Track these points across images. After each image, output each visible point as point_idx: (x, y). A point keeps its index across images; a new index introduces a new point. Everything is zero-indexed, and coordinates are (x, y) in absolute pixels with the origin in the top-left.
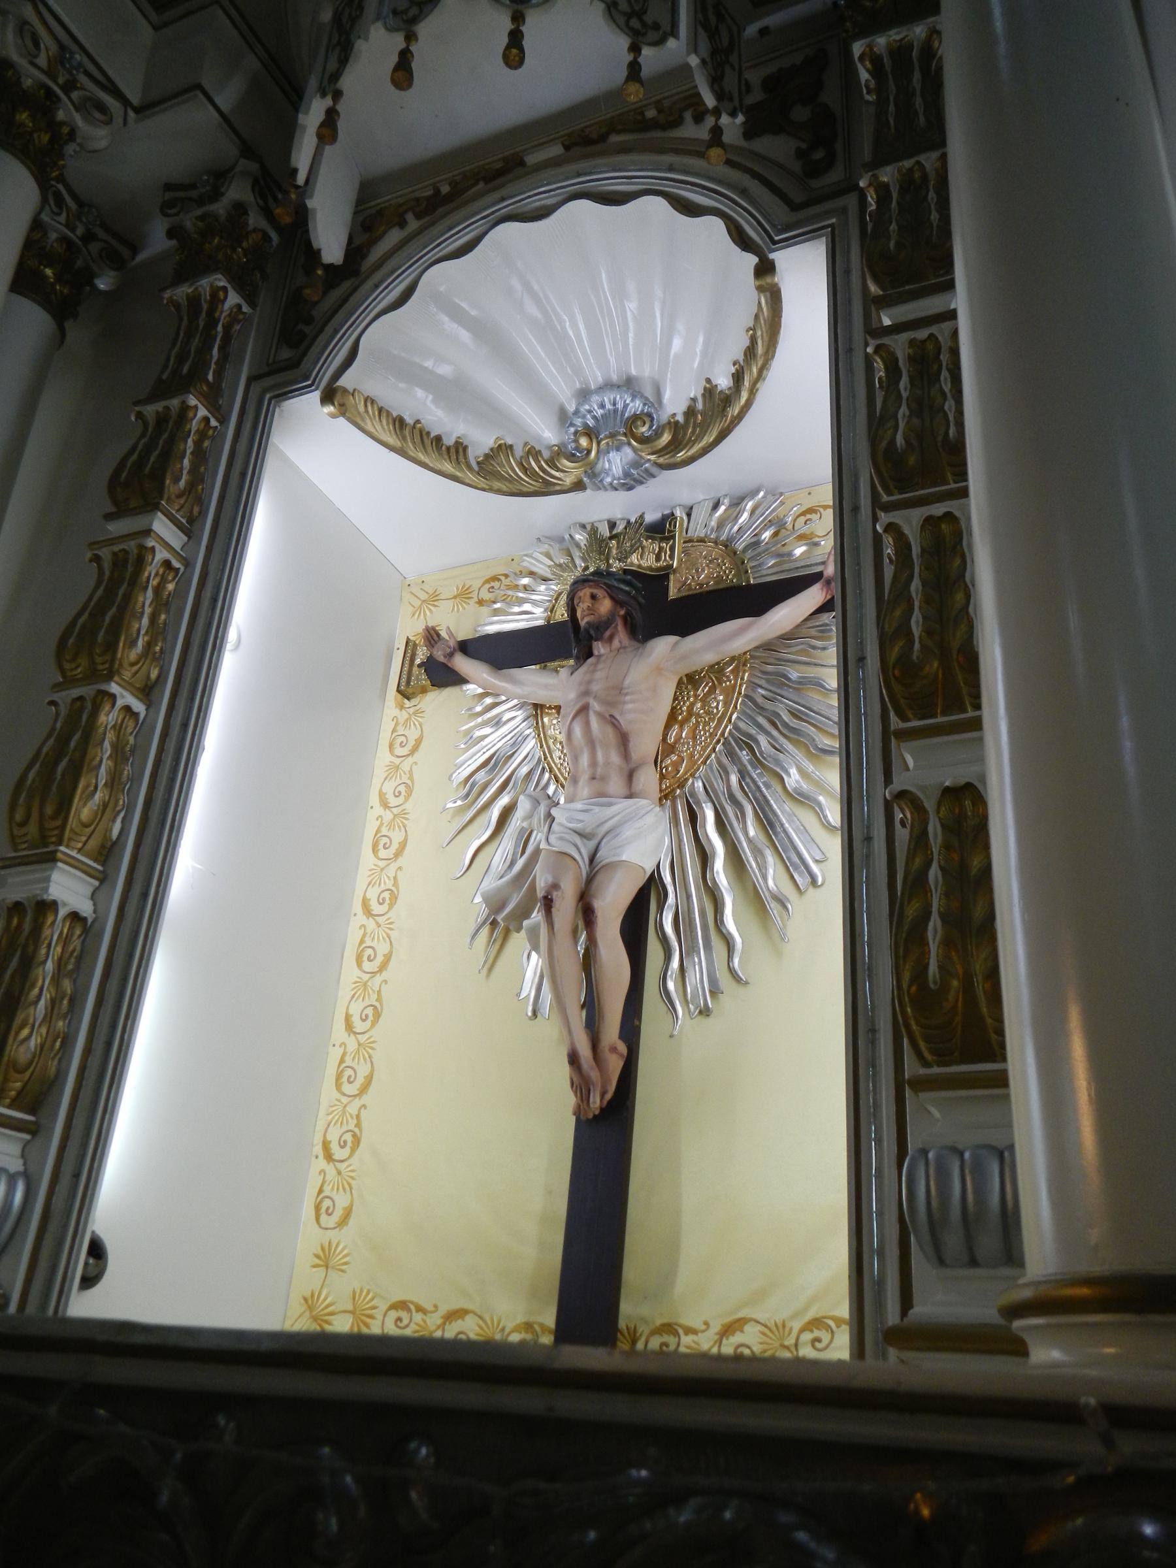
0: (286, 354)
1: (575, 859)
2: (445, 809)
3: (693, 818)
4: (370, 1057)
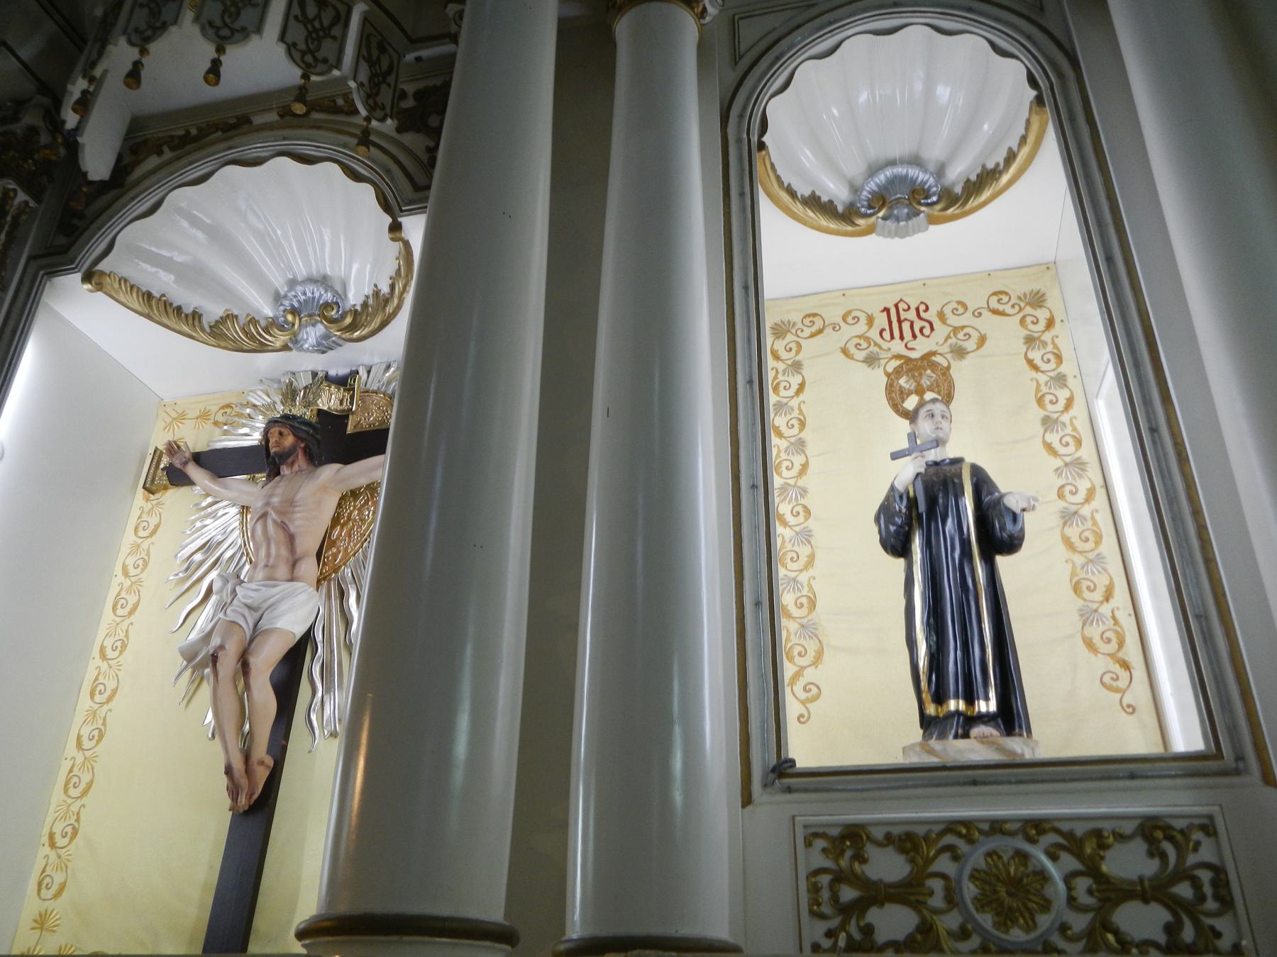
0: (62, 240)
1: (241, 626)
2: (168, 581)
3: (342, 594)
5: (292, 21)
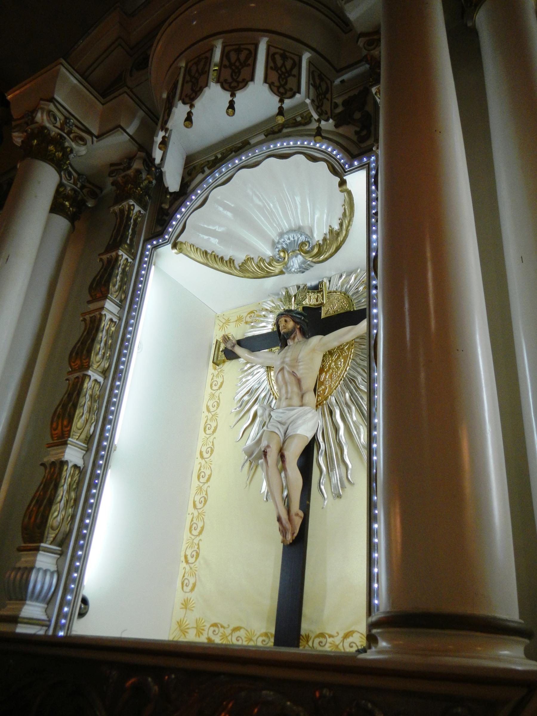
0: (159, 229)
2: (231, 412)
3: (331, 413)
4: (203, 519)
5: (269, 70)
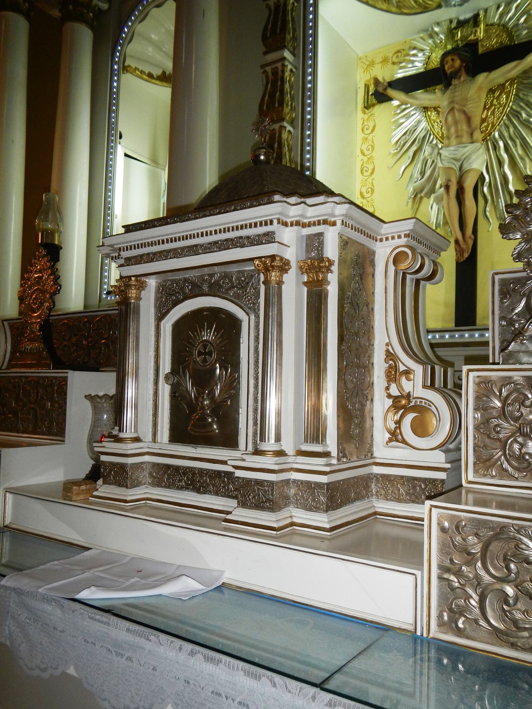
2: (390, 153)
3: (496, 147)
